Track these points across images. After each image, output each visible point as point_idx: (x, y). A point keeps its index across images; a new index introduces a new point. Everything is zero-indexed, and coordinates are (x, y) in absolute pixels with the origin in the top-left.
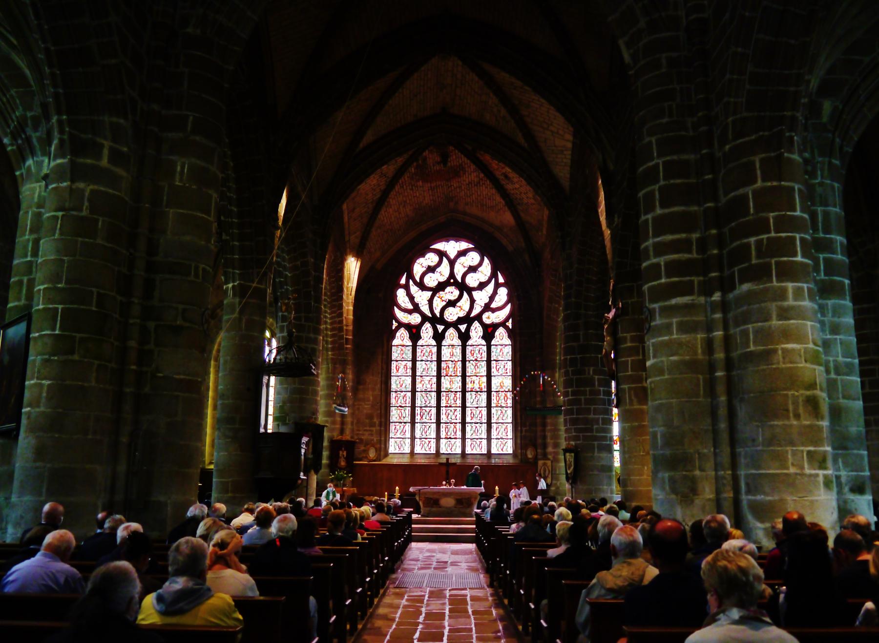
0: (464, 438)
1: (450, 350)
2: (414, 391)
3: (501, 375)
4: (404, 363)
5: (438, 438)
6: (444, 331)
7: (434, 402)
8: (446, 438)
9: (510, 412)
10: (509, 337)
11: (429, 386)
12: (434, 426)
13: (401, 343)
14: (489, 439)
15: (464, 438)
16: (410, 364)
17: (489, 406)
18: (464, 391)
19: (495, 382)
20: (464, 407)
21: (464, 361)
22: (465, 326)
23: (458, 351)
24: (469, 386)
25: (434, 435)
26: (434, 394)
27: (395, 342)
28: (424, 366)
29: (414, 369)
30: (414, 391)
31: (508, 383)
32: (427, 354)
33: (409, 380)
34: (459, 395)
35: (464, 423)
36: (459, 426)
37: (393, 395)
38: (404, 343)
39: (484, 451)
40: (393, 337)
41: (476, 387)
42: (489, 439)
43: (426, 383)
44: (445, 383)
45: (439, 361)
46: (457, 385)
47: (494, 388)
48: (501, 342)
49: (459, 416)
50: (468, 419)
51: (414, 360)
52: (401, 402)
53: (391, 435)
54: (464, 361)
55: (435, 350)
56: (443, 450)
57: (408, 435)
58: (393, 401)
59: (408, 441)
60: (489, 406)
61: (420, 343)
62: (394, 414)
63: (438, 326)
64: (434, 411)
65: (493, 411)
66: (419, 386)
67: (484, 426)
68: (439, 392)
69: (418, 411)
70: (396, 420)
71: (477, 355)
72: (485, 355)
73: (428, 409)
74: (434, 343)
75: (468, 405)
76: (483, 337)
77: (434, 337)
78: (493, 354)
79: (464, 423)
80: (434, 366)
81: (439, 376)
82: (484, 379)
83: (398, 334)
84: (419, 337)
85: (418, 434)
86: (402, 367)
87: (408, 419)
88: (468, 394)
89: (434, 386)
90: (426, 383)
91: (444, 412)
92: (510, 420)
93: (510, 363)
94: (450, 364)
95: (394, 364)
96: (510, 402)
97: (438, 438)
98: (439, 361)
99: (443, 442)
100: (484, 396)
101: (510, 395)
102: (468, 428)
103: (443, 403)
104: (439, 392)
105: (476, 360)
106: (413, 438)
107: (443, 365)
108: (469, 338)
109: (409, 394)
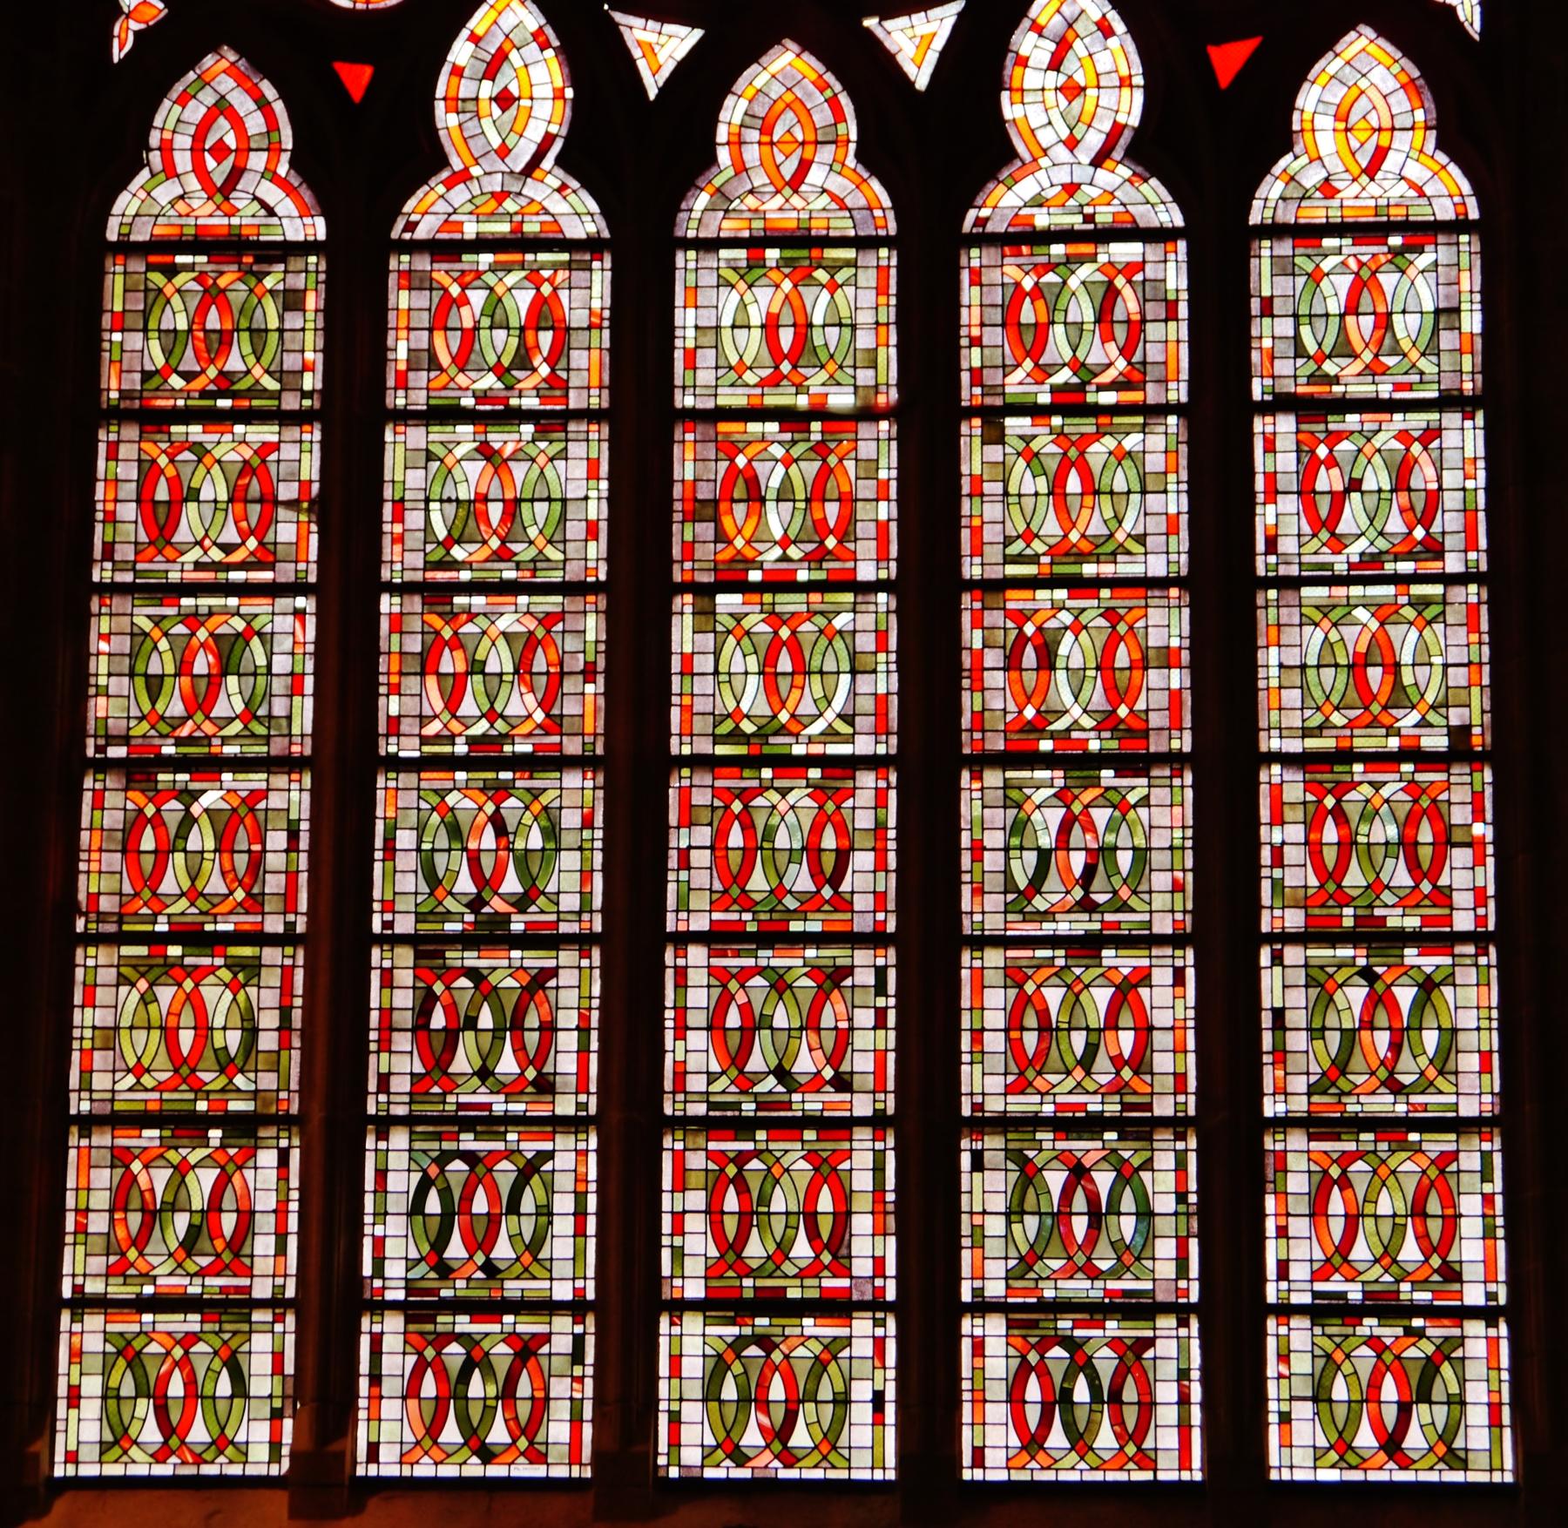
0: (929, 1313)
1: (763, 300)
2: (347, 760)
3: (1368, 571)
4: (233, 445)
5: (629, 1303)
6: (705, 80)
7: (574, 885)
8: (714, 1305)
9: (1472, 1000)
10: (1455, 138)
11: (520, 703)
12: (573, 1161)
13: (205, 213)
14: (1233, 1313)
15: (929, 1313)
16: (302, 458)
17: (1225, 934)
18: (930, 752)
19: (1295, 656)
20: (929, 939)
21: (931, 407)
22: (939, 24)
23: (858, 306)
24: (991, 699)
25: (570, 1264)
26: (576, 792)
27: (141, 206)
28: (472, 476)
29: (351, 504)
30: (347, 760)
31: (1446, 661)
32: (499, 344)
33: (289, 634)
34: (870, 803)
35: (929, 1125)
36: (866, 1163)
37: (106, 807)
38: (246, 215)
39: (1174, 1452)
40: (125, 155)
41: (1075, 707)
42: (1233, 1313)
43: (497, 671)
44: (717, 673)
45: (643, 410)
46: (848, 695)
47: (1283, 723)
48: (1358, 199)
49: (872, 1047)
50: (983, 1083)
51: (353, 413)
52: (193, 878)
53: (81, 1267)
54: (931, 407)
55: (591, 293)
56: (690, 1442)
57: (272, 1266)
58: (100, 878)
59: (268, 1348)
60: (1225, 934)
61: (428, 210)
62: (118, 1032)
63: (637, 31)
64: (577, 985)
65: (1279, 986)
66: (408, 708)
67: (1167, 1174)
68: (635, 763)
69: (394, 985)
70: (128, 1093)
71: (1076, 345)
72: (1169, 342)
73: (505, 969)
74: (579, 214)
75: (984, 911)
76: (1147, 149)
77: (585, 153)
78: (1268, 333)
79: (929, 1125)
80: (578, 474)
81: (640, 586)
82: (1168, 624)
83: (175, 120)
84: (425, 158)
85: (393, 1248)
86: (215, 488)
87: (277, 1080)
88: (978, 803)
89: (585, 701)
90: (497, 671)
91: (698, 997)
92: (1475, 1093)
93: (1465, 438)
94: (774, 459)
95: (119, 463)
96: (1469, 879)
97: (629, 1303)
98: (643, 410)
99: (690, 1342)
100: (1165, 813)
101: (1465, 796)
102: (985, 1191)
103: (692, 901)
104: (635, 763)
105: (1070, 403)
106: (332, 1300)
107: (690, 464)
108: (995, 153)
109: (292, 797)
